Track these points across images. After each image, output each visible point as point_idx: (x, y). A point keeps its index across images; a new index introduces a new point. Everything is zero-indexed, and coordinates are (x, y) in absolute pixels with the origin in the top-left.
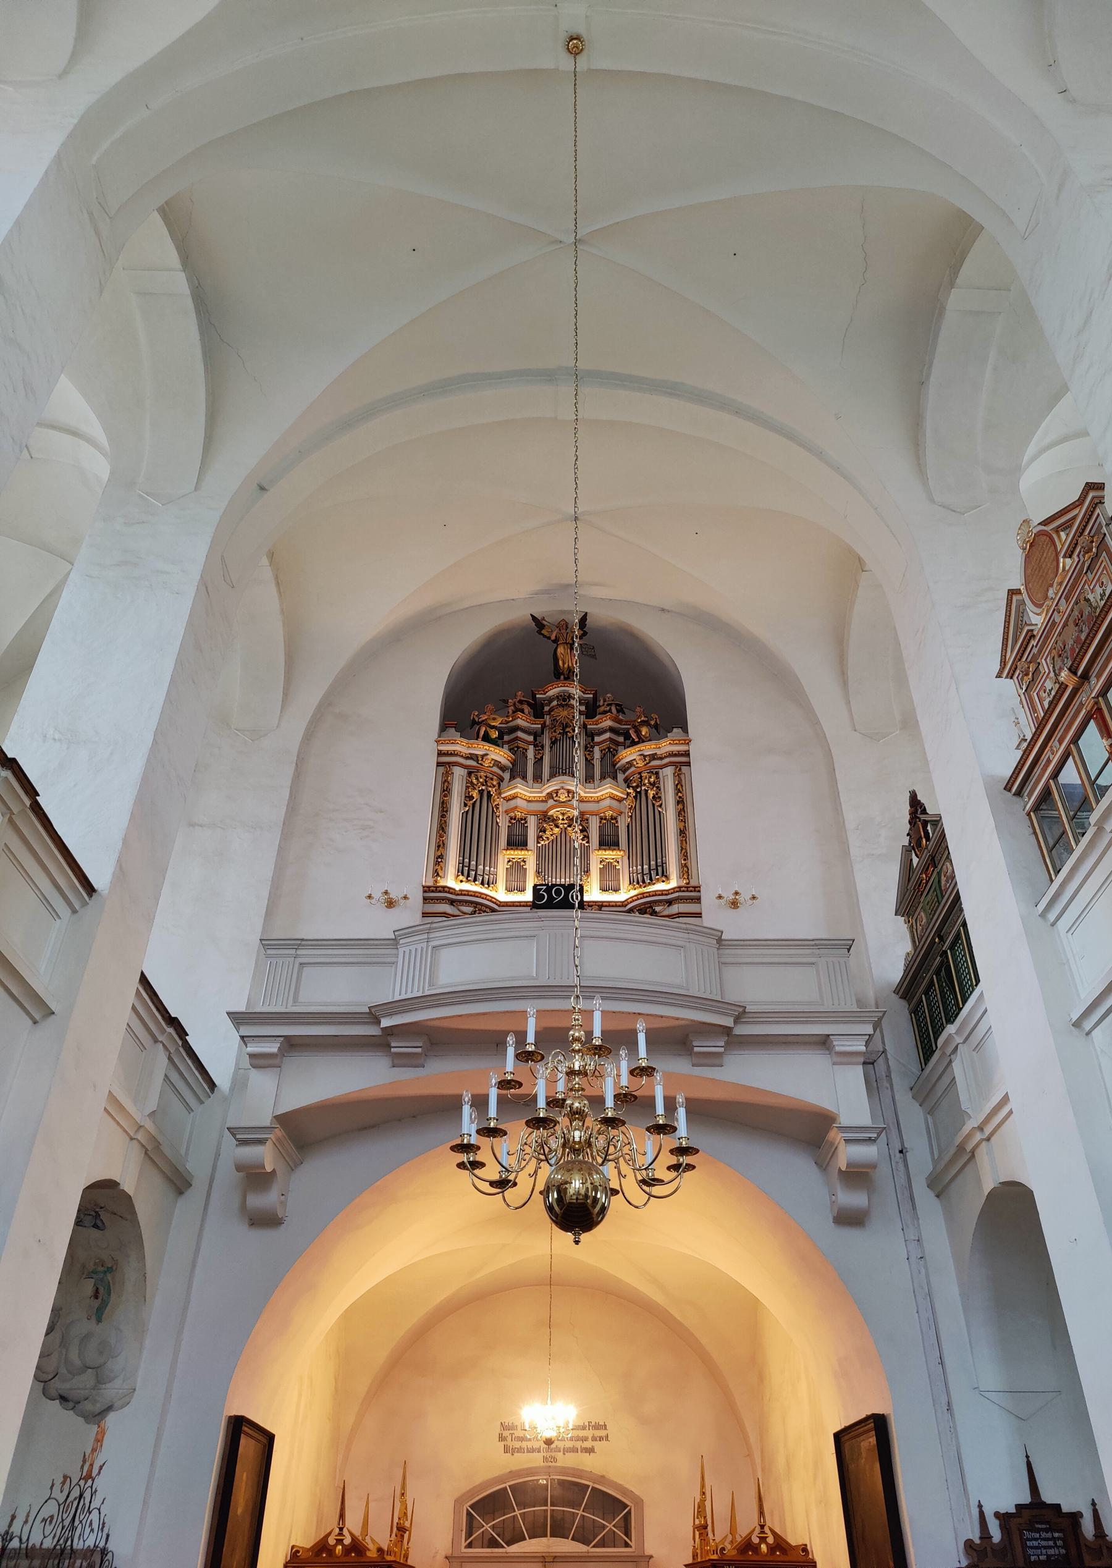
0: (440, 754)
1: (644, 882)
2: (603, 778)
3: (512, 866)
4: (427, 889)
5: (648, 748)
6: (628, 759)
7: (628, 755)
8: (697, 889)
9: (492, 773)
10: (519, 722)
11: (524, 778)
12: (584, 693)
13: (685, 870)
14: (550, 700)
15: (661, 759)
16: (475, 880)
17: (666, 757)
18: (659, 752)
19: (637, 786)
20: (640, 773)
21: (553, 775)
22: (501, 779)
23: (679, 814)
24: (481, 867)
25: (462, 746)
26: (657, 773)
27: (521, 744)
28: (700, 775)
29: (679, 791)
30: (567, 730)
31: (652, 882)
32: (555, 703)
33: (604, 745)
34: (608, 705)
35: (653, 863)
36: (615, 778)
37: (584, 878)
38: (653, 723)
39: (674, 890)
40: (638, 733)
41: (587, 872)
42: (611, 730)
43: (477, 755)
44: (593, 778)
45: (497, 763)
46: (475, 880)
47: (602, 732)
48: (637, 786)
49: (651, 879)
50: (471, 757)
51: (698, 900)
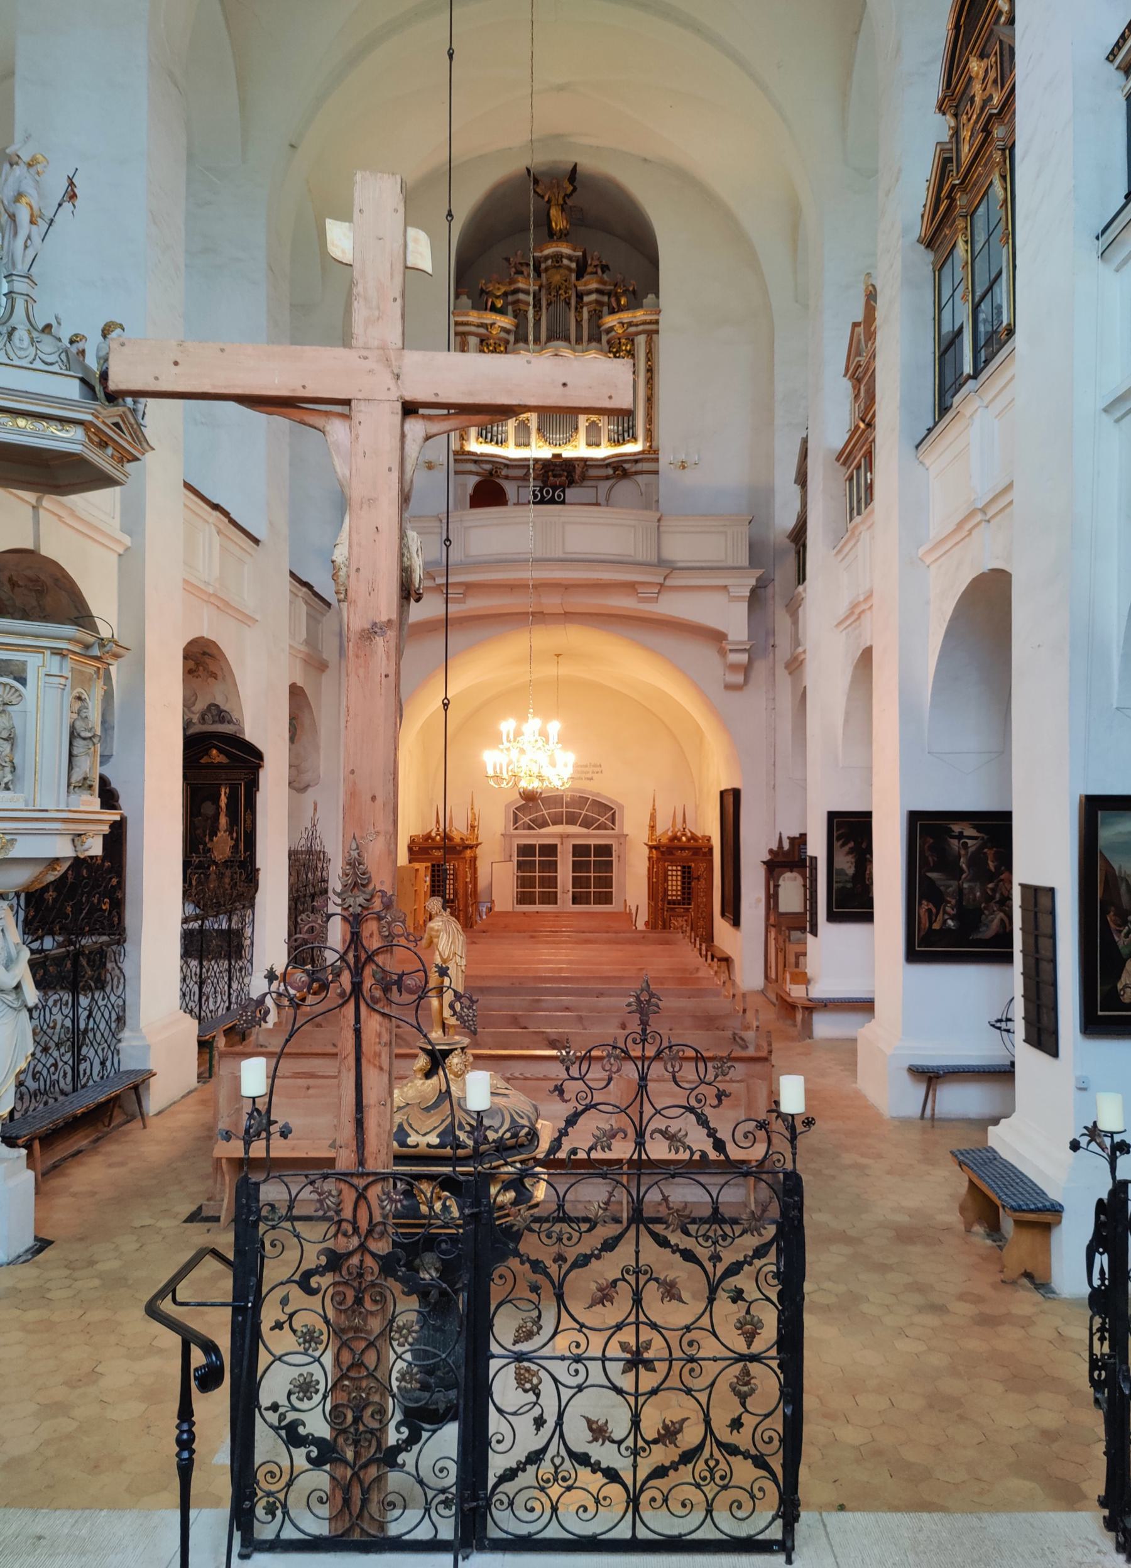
0: (457, 324)
1: (618, 441)
2: (590, 340)
3: (519, 424)
4: (456, 453)
5: (626, 316)
6: (610, 325)
7: (610, 321)
8: (656, 452)
9: (500, 339)
10: (521, 285)
11: (526, 341)
12: (574, 251)
13: (650, 435)
14: (546, 258)
15: (637, 325)
16: (491, 440)
17: (641, 324)
18: (635, 320)
19: (617, 352)
20: (619, 339)
21: (550, 339)
22: (507, 342)
23: (648, 382)
24: (495, 429)
25: (474, 317)
26: (633, 340)
27: (522, 307)
28: (664, 341)
29: (649, 360)
30: (561, 292)
31: (624, 442)
32: (549, 262)
33: (593, 306)
34: (596, 266)
35: (626, 425)
36: (599, 341)
37: (574, 434)
38: (631, 289)
39: (642, 452)
40: (618, 301)
41: (576, 429)
42: (599, 291)
43: (486, 324)
44: (582, 339)
45: (504, 329)
46: (491, 440)
47: (589, 293)
48: (617, 352)
49: (624, 440)
50: (482, 326)
51: (657, 460)
